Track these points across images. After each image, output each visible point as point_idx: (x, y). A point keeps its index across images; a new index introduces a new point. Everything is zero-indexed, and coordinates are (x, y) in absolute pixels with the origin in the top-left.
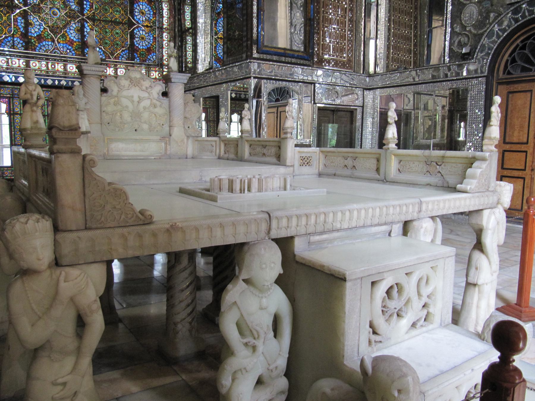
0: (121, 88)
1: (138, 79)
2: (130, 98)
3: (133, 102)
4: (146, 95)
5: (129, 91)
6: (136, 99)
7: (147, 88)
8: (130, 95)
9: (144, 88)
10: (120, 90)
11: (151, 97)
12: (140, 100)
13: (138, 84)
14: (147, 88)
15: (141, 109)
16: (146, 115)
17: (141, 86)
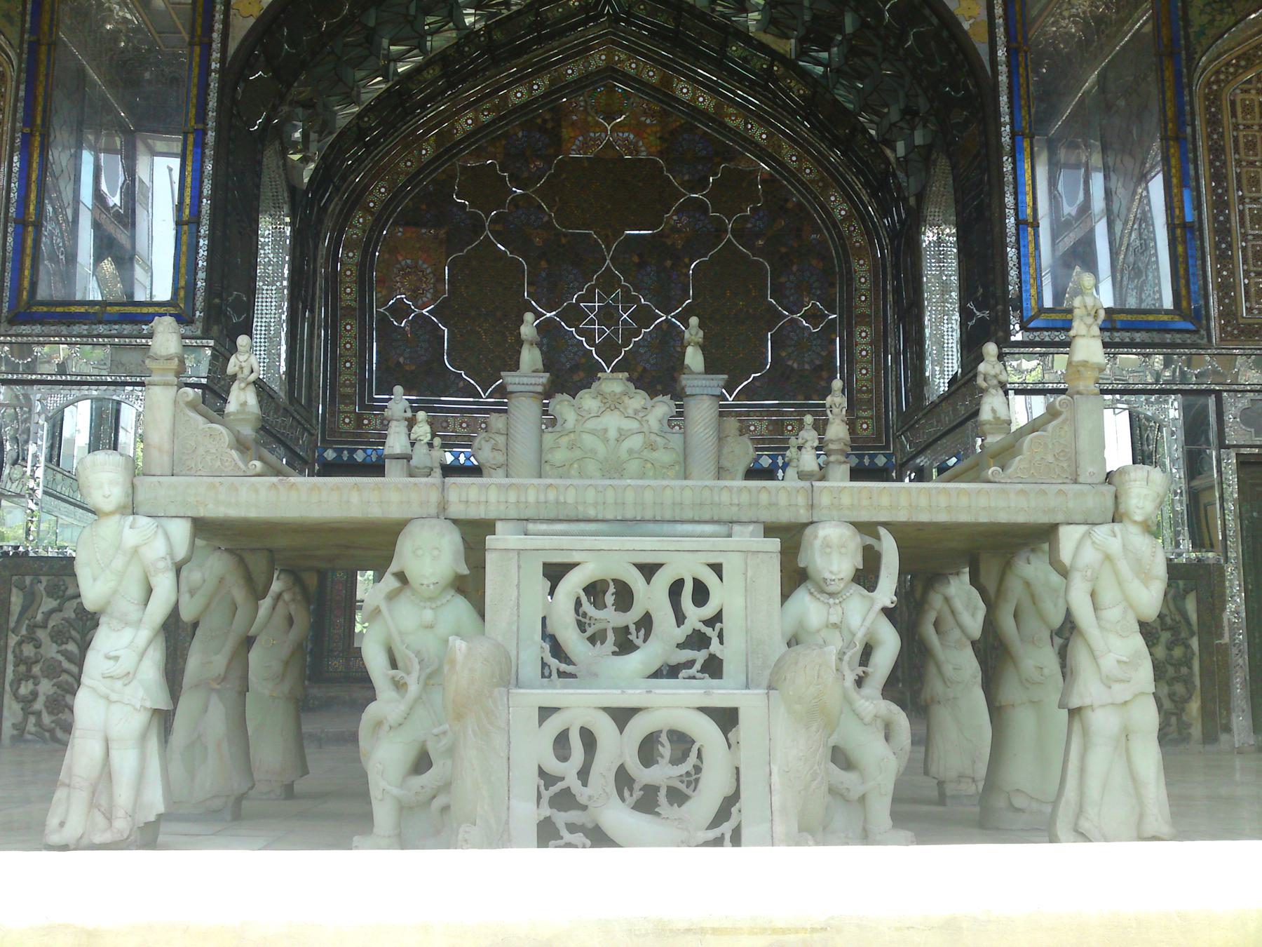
0: (584, 414)
1: (617, 397)
2: (602, 434)
3: (606, 440)
4: (634, 425)
5: (599, 419)
6: (612, 434)
7: (636, 412)
8: (599, 427)
9: (631, 412)
10: (580, 418)
11: (645, 429)
12: (622, 435)
13: (617, 404)
14: (636, 412)
15: (624, 454)
17: (625, 408)
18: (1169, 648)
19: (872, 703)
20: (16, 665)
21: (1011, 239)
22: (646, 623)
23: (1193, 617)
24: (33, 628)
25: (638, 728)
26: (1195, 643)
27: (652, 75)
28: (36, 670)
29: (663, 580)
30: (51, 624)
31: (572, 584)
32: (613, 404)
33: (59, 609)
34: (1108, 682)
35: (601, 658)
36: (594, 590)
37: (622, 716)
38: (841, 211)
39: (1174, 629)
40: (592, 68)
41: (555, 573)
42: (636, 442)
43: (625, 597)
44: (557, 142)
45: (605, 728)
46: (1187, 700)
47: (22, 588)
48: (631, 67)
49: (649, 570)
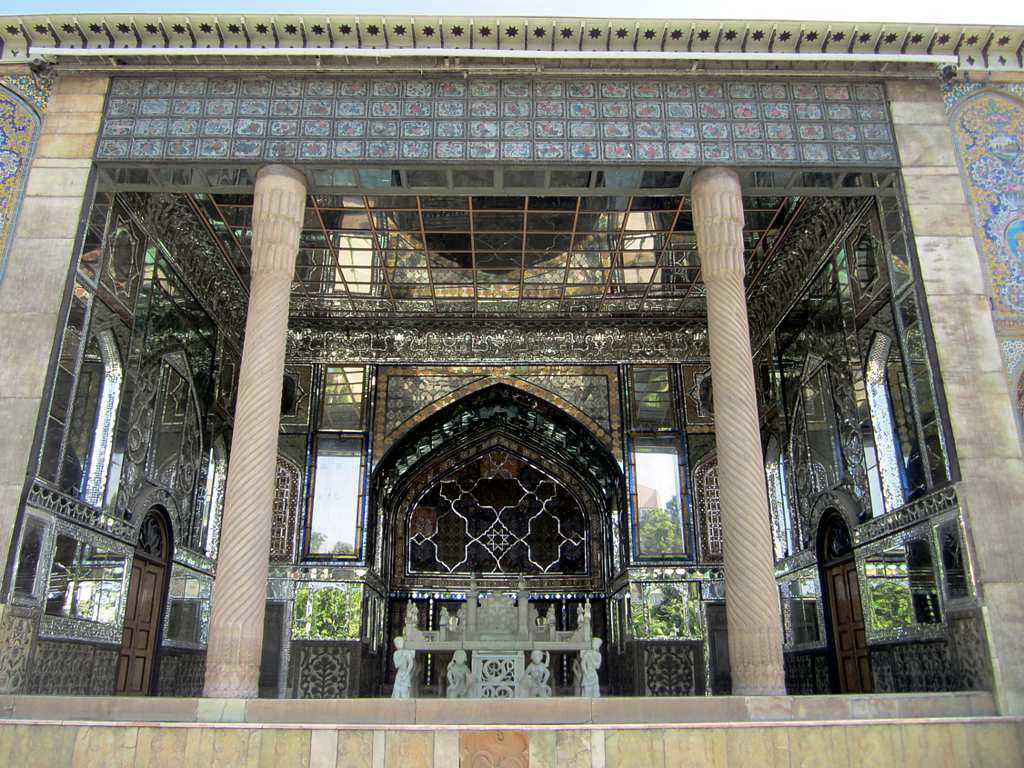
2: (494, 609)
4: (503, 606)
12: (500, 609)
16: (503, 619)
18: (685, 669)
19: (544, 685)
20: (302, 677)
21: (630, 531)
22: (500, 671)
23: (692, 659)
24: (308, 664)
25: (498, 689)
26: (693, 668)
27: (514, 447)
28: (309, 679)
29: (504, 663)
30: (314, 663)
31: (487, 664)
32: (497, 599)
33: (317, 658)
34: (588, 681)
35: (492, 677)
36: (491, 665)
37: (496, 687)
38: (586, 498)
39: (686, 663)
40: (492, 444)
41: (484, 662)
42: (503, 611)
43: (497, 666)
44: (478, 473)
45: (493, 690)
46: (690, 688)
47: (304, 650)
48: (506, 444)
49: (501, 661)
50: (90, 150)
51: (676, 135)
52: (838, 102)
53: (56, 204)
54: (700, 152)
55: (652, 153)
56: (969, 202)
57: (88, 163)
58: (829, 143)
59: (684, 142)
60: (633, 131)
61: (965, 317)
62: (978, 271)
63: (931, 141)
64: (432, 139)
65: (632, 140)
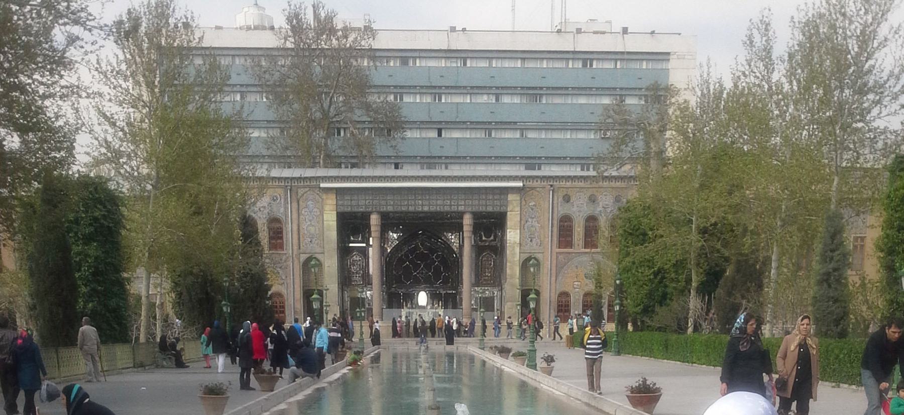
50: (335, 209)
51: (460, 203)
52: (497, 194)
53: (331, 223)
54: (465, 208)
55: (454, 208)
56: (521, 219)
57: (335, 212)
58: (493, 206)
59: (461, 205)
60: (451, 202)
61: (514, 247)
62: (519, 238)
63: (515, 205)
64: (408, 205)
65: (451, 205)
